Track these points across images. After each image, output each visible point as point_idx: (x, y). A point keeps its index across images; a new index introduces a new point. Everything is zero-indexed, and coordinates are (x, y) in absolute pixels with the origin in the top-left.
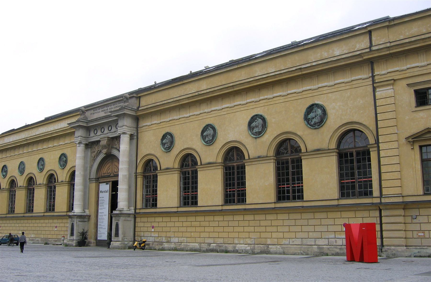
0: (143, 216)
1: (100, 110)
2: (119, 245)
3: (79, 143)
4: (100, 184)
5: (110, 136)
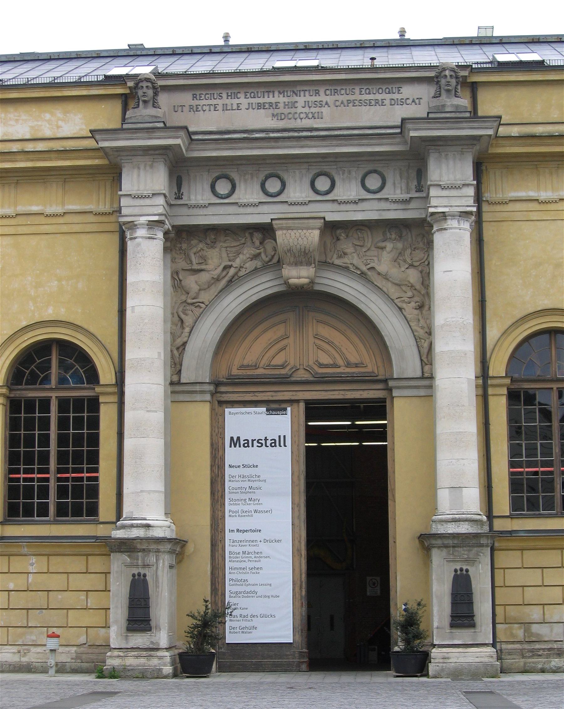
0: (531, 544)
2: (486, 660)
3: (152, 225)
4: (227, 410)
5: (330, 217)
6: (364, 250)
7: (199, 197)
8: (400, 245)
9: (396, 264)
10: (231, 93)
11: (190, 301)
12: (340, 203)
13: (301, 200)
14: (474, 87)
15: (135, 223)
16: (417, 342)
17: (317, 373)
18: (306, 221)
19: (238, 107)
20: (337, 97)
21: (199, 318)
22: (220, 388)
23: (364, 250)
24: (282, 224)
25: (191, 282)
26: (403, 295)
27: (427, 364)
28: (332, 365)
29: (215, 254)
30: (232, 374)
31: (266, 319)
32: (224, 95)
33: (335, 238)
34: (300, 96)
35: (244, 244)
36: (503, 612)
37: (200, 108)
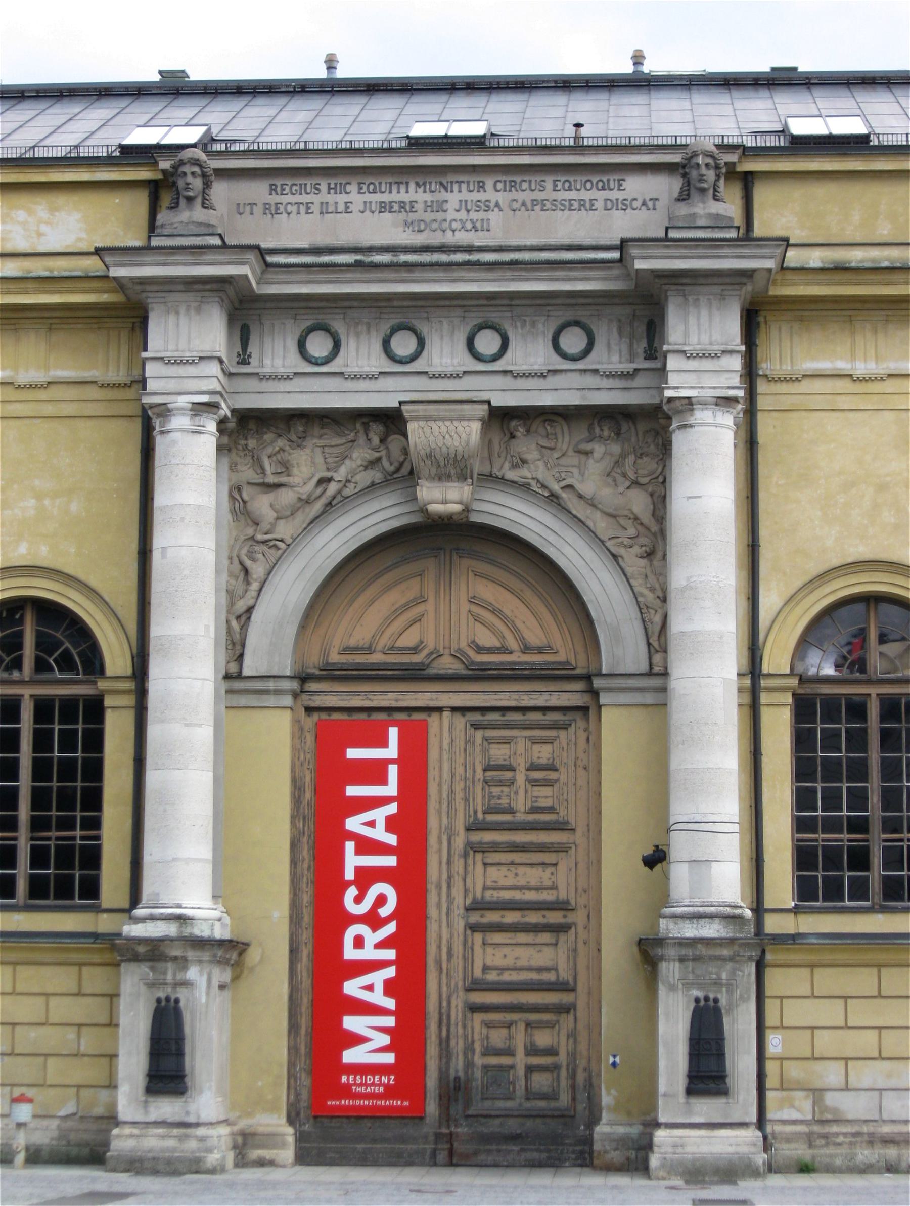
0: (827, 957)
1: (342, 198)
3: (199, 409)
5: (499, 400)
6: (556, 455)
7: (278, 362)
8: (616, 448)
9: (610, 480)
10: (336, 184)
11: (259, 537)
12: (516, 375)
13: (450, 369)
14: (747, 180)
15: (169, 405)
16: (641, 613)
17: (473, 663)
18: (458, 407)
19: (347, 208)
20: (514, 194)
21: (275, 565)
22: (310, 684)
23: (556, 455)
24: (417, 411)
25: (263, 505)
26: (619, 533)
27: (657, 651)
28: (498, 649)
29: (304, 457)
30: (330, 661)
31: (387, 570)
32: (324, 187)
33: (508, 435)
34: (452, 191)
35: (353, 441)
36: (778, 1071)
37: (282, 208)
